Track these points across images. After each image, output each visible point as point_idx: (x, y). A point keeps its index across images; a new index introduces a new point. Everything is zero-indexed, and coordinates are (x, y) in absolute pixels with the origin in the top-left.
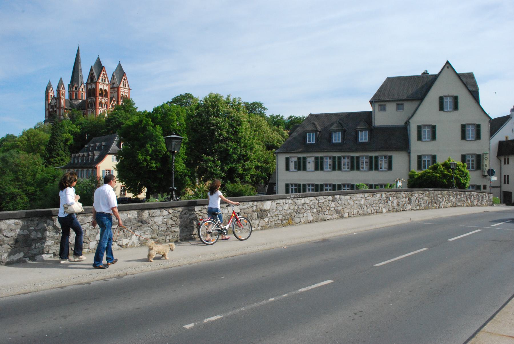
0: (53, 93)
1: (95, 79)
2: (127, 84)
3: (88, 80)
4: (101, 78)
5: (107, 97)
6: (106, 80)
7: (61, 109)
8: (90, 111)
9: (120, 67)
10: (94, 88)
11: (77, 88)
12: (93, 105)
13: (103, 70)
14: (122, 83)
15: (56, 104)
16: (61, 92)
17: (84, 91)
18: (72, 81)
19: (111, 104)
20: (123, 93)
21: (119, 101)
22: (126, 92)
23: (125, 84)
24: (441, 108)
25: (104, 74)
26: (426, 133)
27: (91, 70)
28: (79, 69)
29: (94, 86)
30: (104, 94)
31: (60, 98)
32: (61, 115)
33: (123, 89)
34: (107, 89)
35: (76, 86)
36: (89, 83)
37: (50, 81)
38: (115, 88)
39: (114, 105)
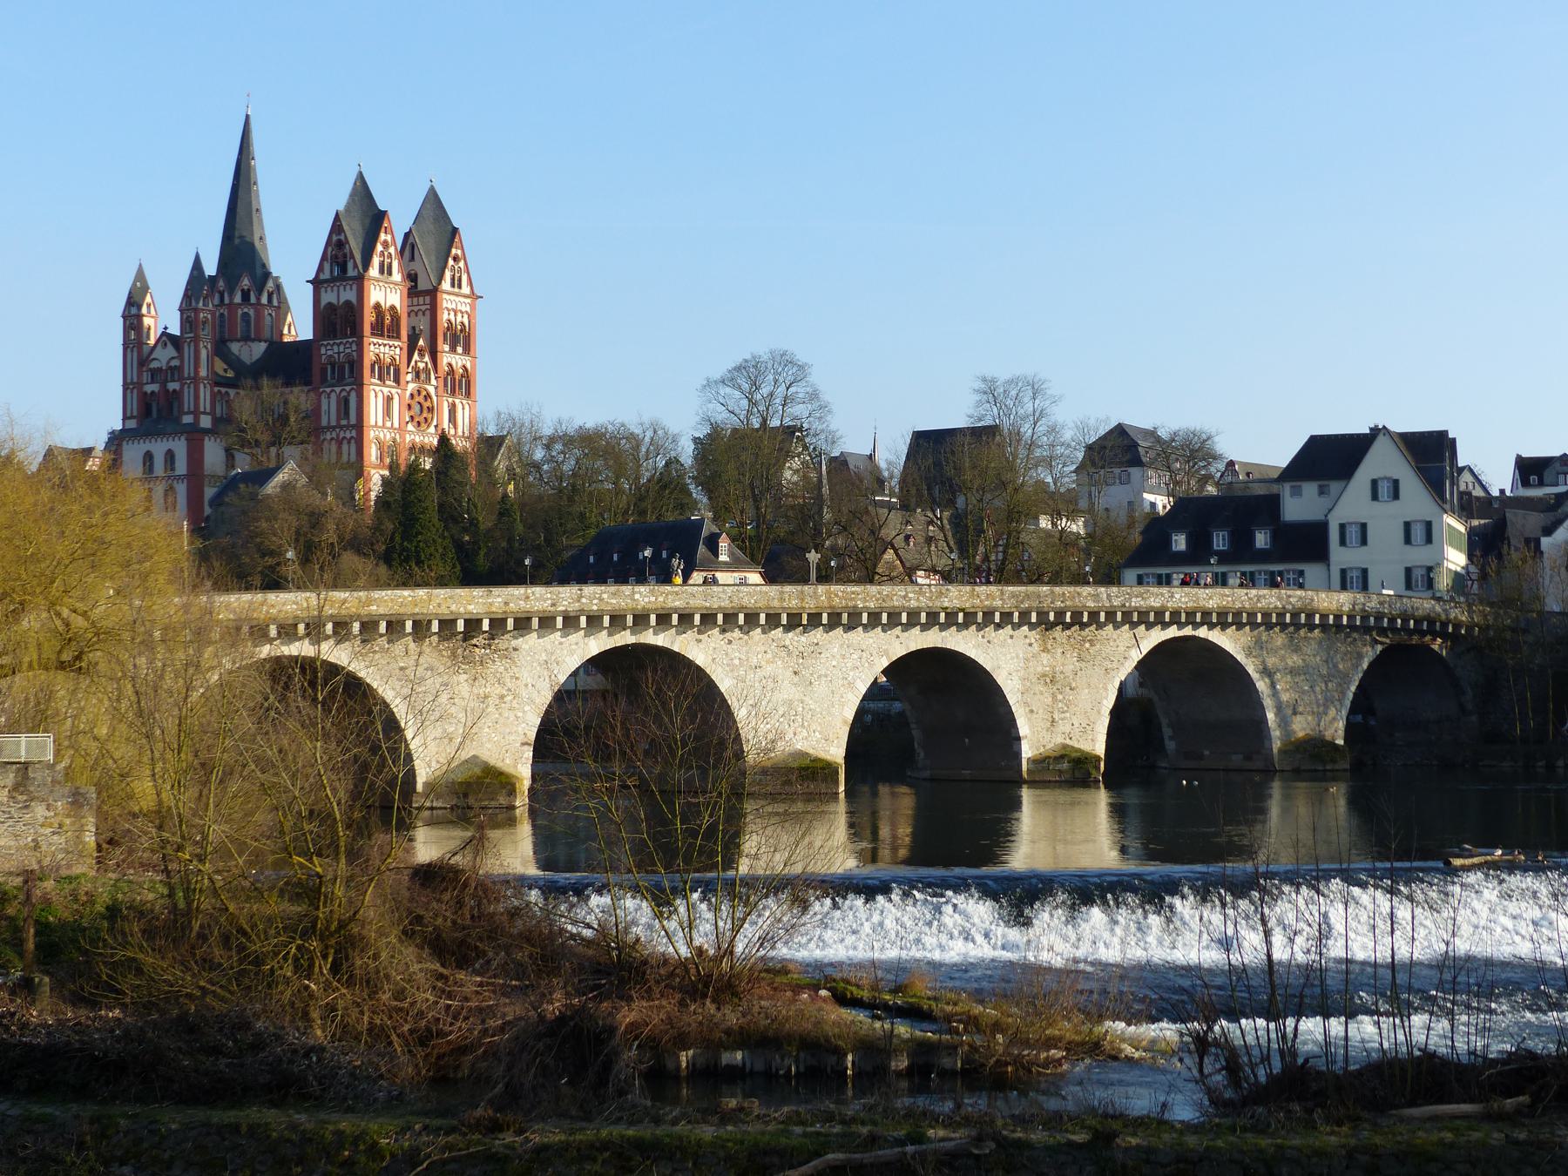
0: (163, 317)
1: (355, 266)
3: (320, 269)
4: (376, 260)
5: (398, 337)
7: (202, 386)
8: (333, 396)
9: (433, 206)
10: (348, 303)
11: (249, 290)
12: (350, 373)
13: (383, 230)
14: (448, 274)
15: (175, 363)
16: (202, 315)
17: (275, 303)
19: (413, 363)
20: (452, 314)
21: (439, 348)
22: (464, 309)
23: (457, 275)
24: (1375, 497)
26: (1353, 533)
27: (337, 227)
28: (254, 210)
29: (349, 295)
30: (386, 325)
31: (196, 340)
32: (202, 410)
33: (452, 297)
34: (399, 308)
35: (246, 282)
36: (326, 281)
37: (140, 265)
38: (422, 294)
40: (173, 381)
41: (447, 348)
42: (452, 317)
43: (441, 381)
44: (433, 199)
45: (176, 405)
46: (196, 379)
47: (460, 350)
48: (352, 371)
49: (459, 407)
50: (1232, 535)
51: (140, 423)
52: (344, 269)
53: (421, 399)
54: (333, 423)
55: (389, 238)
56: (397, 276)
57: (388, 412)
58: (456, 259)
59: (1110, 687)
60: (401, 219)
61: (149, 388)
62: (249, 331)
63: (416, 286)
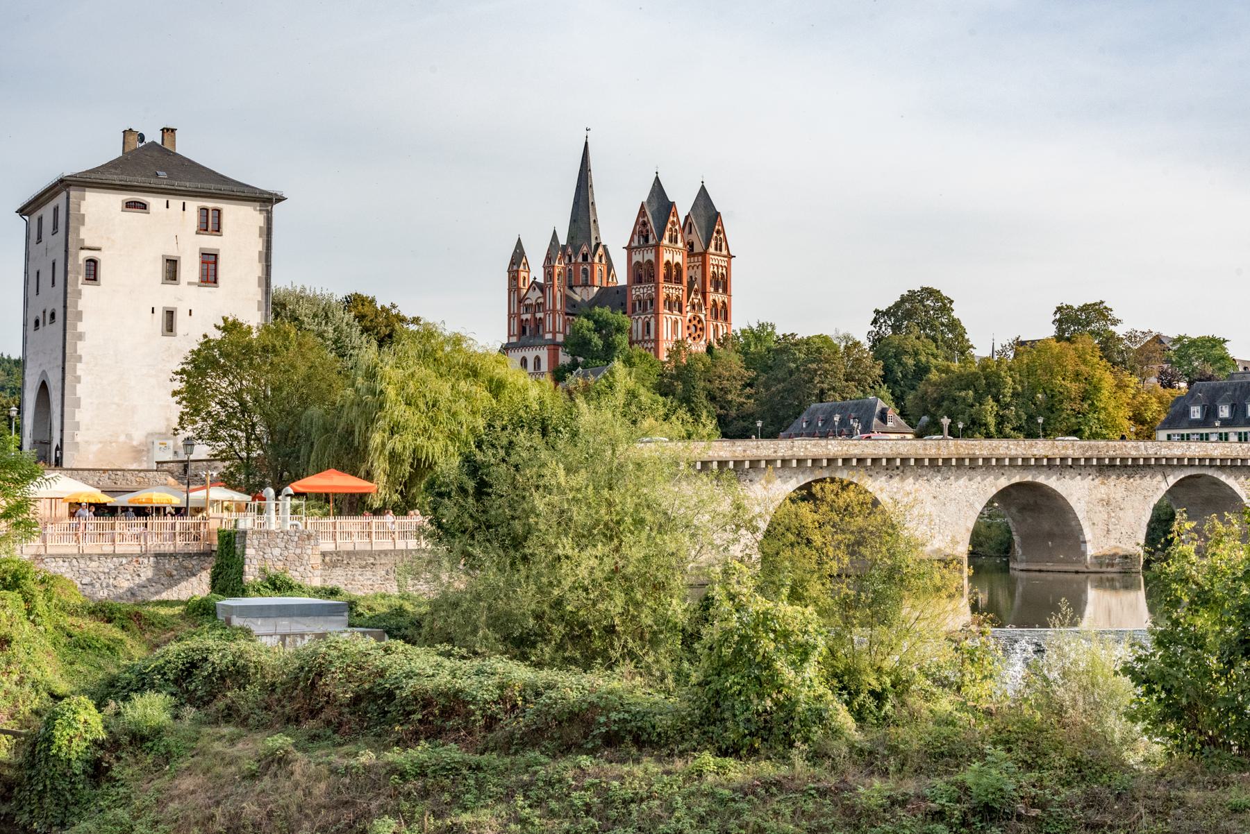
2: (724, 244)
3: (632, 240)
4: (667, 234)
5: (681, 283)
6: (679, 236)
10: (649, 261)
12: (649, 305)
14: (713, 243)
15: (539, 301)
17: (604, 262)
18: (571, 237)
25: (673, 222)
27: (642, 212)
29: (650, 256)
30: (674, 273)
35: (585, 248)
36: (636, 248)
39: (696, 301)
40: (539, 312)
41: (712, 290)
42: (716, 270)
43: (709, 311)
44: (703, 194)
45: (541, 327)
46: (554, 311)
47: (720, 291)
48: (652, 304)
49: (720, 328)
50: (1232, 406)
51: (519, 339)
52: (647, 240)
53: (695, 322)
54: (640, 338)
55: (675, 219)
56: (680, 245)
57: (675, 331)
58: (718, 232)
59: (1146, 507)
60: (684, 208)
61: (524, 317)
62: (587, 280)
63: (692, 250)
